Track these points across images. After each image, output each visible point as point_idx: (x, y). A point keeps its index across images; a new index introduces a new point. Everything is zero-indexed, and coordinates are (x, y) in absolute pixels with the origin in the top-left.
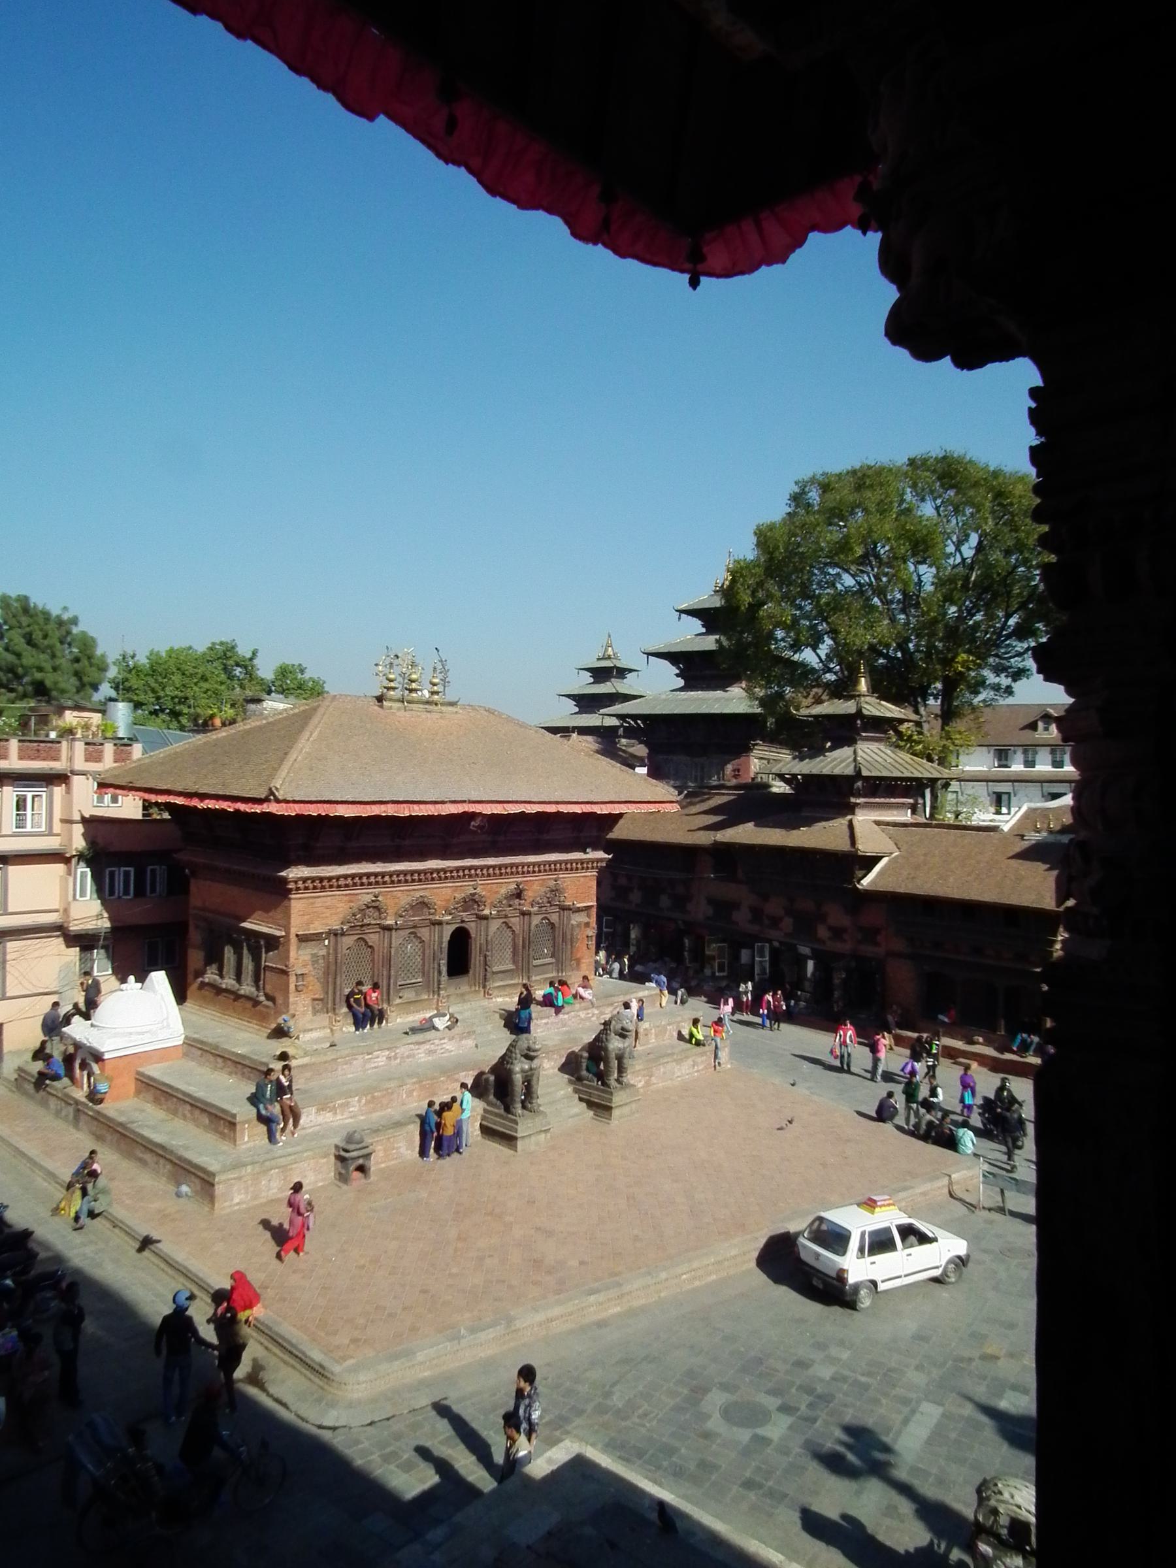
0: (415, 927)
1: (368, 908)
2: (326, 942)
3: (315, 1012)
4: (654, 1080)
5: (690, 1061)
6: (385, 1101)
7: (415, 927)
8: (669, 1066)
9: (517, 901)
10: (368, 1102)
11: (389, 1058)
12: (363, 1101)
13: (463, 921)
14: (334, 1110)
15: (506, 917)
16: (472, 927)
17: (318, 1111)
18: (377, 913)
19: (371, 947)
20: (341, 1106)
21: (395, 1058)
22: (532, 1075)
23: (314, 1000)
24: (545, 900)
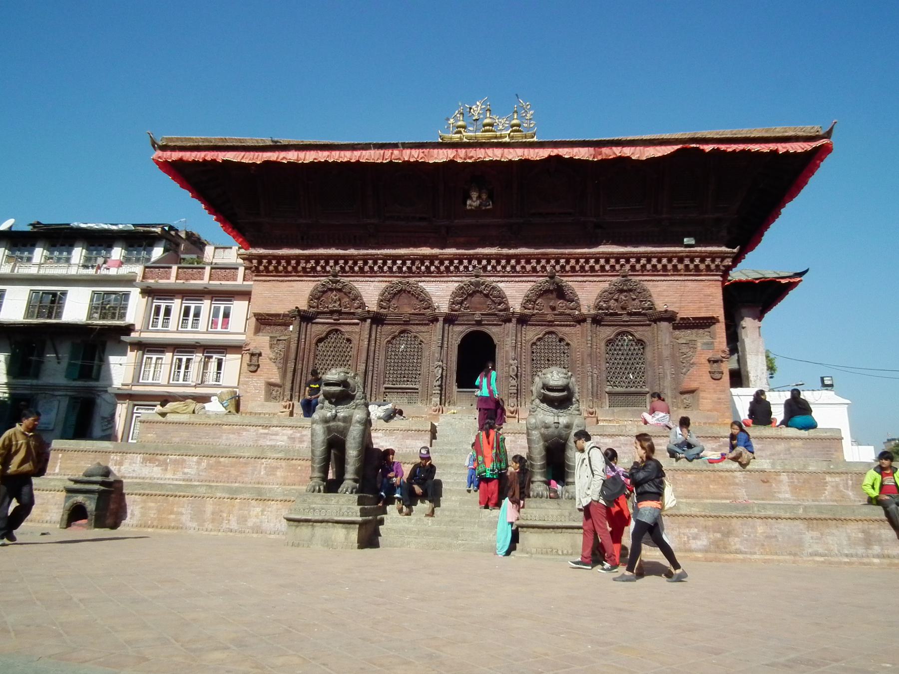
0: (407, 323)
1: (331, 290)
2: (291, 328)
3: (269, 397)
4: (735, 543)
5: (853, 530)
6: (234, 472)
7: (407, 323)
8: (784, 525)
9: (560, 303)
10: (210, 467)
11: (292, 439)
12: (204, 464)
13: (479, 323)
14: (164, 465)
15: (550, 323)
16: (494, 331)
17: (144, 461)
18: (346, 300)
19: (349, 340)
20: (175, 462)
21: (301, 442)
22: (344, 432)
23: (270, 385)
24: (612, 303)
